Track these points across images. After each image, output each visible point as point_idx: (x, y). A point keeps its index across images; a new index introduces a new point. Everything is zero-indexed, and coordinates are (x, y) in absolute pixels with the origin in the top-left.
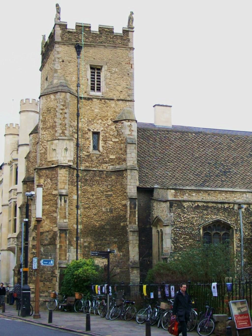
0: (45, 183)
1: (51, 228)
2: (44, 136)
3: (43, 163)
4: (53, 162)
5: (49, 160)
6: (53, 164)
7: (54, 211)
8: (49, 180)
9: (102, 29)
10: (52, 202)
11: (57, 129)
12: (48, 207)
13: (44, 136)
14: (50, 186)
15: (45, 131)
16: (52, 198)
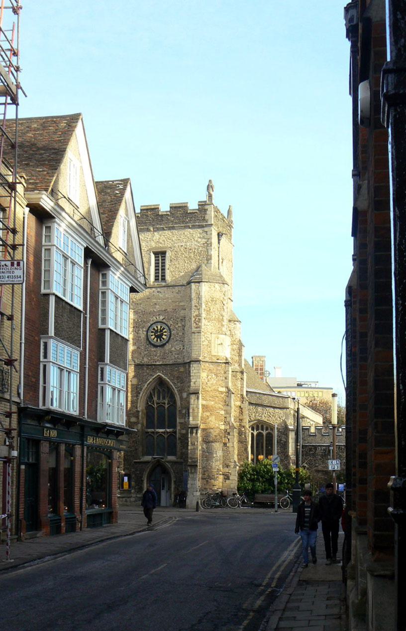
0: (209, 377)
1: (217, 425)
2: (208, 327)
3: (205, 356)
4: (218, 358)
5: (213, 353)
6: (218, 359)
7: (220, 408)
8: (213, 375)
9: (175, 208)
10: (217, 399)
11: (224, 323)
12: (213, 403)
13: (208, 327)
14: (215, 382)
15: (209, 322)
16: (218, 395)
